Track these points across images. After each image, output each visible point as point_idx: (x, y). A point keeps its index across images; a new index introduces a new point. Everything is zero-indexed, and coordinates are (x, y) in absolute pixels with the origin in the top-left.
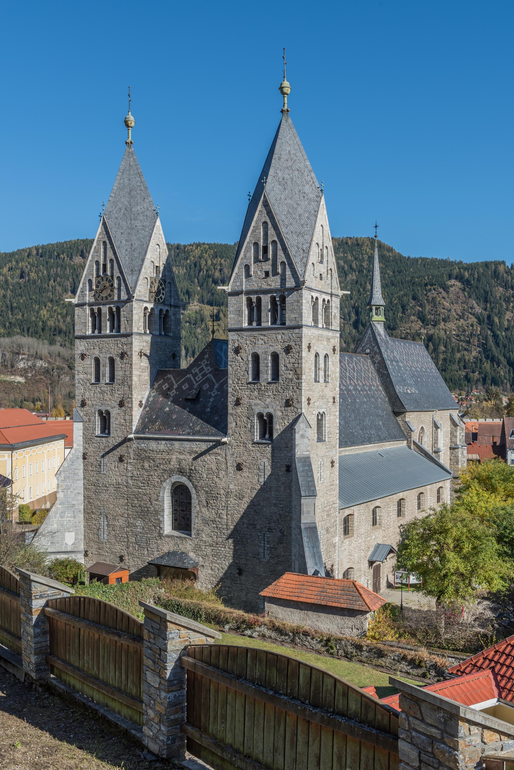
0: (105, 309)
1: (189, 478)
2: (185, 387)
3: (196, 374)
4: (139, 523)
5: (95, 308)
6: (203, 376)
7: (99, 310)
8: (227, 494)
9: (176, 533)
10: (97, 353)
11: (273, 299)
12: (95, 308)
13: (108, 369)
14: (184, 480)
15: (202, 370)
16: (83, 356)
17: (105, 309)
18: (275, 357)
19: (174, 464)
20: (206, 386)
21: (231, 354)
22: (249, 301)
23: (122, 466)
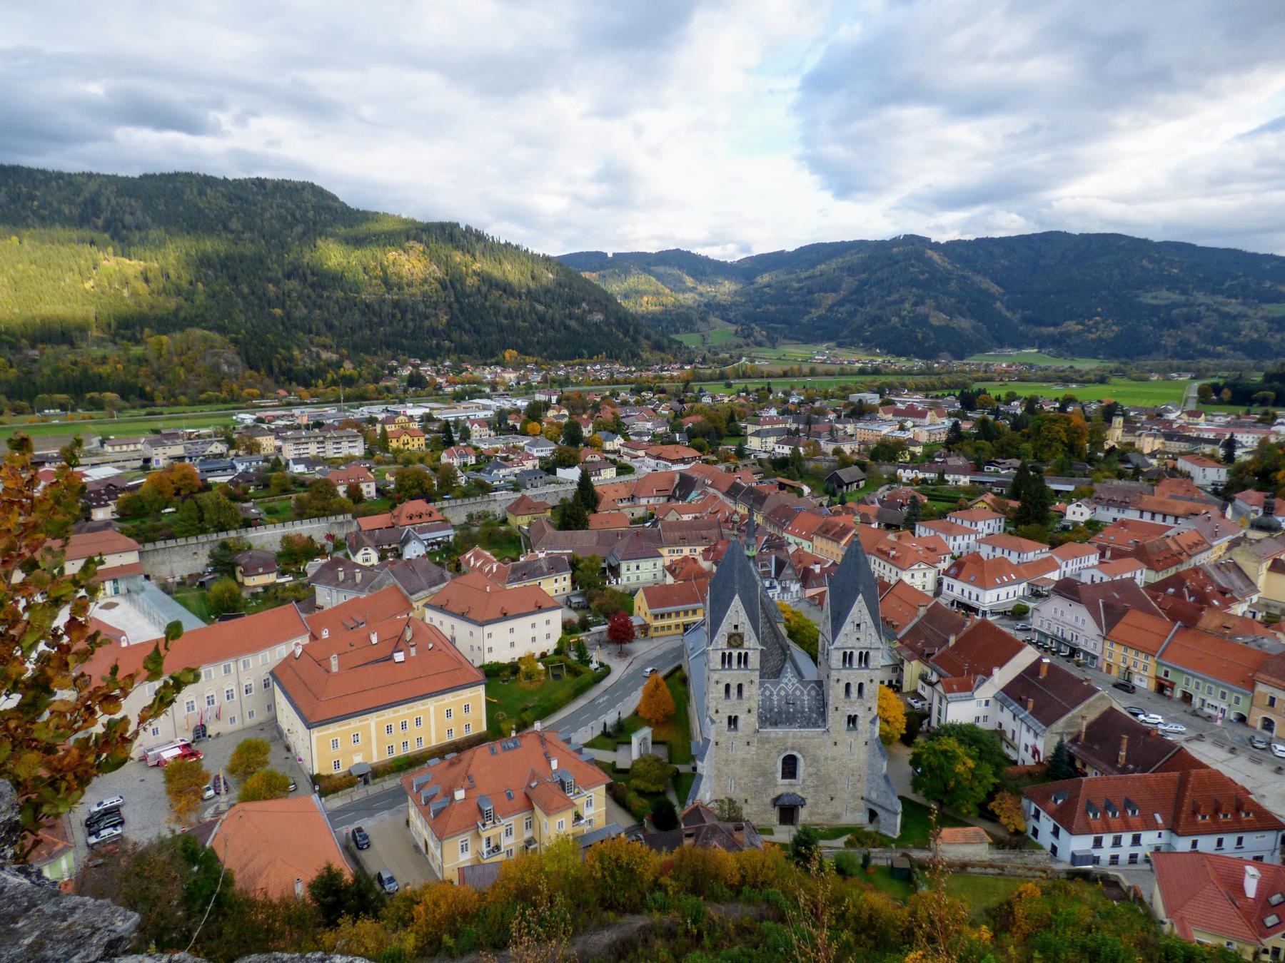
0: (735, 654)
1: (800, 752)
2: (783, 693)
3: (787, 684)
4: (760, 780)
5: (727, 652)
6: (793, 684)
7: (730, 654)
8: (826, 759)
9: (787, 781)
10: (728, 681)
11: (861, 653)
12: (727, 652)
13: (736, 691)
14: (795, 753)
15: (790, 680)
16: (717, 682)
17: (735, 654)
18: (861, 685)
19: (789, 745)
20: (798, 693)
21: (832, 683)
22: (845, 653)
23: (747, 748)
